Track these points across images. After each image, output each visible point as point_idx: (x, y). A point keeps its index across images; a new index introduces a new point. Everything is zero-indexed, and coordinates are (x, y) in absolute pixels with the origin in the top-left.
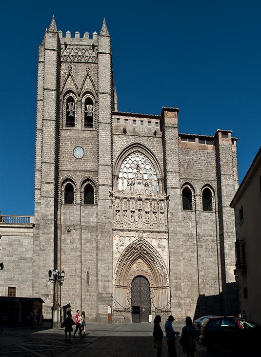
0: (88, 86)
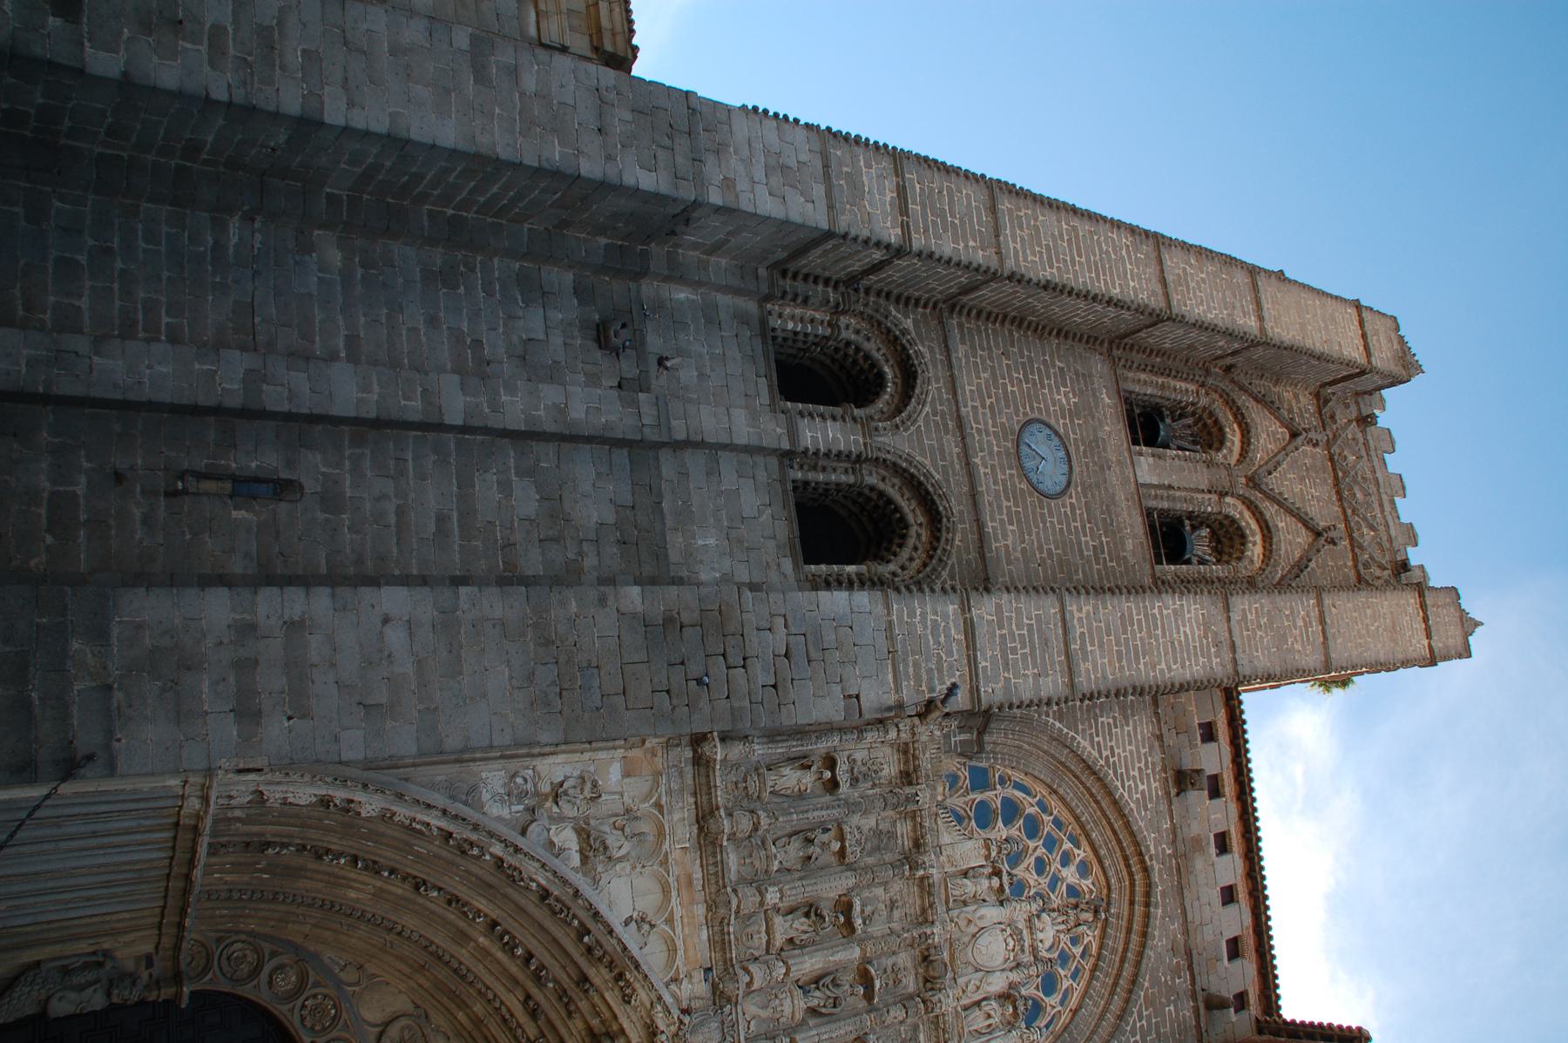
0: (1291, 539)
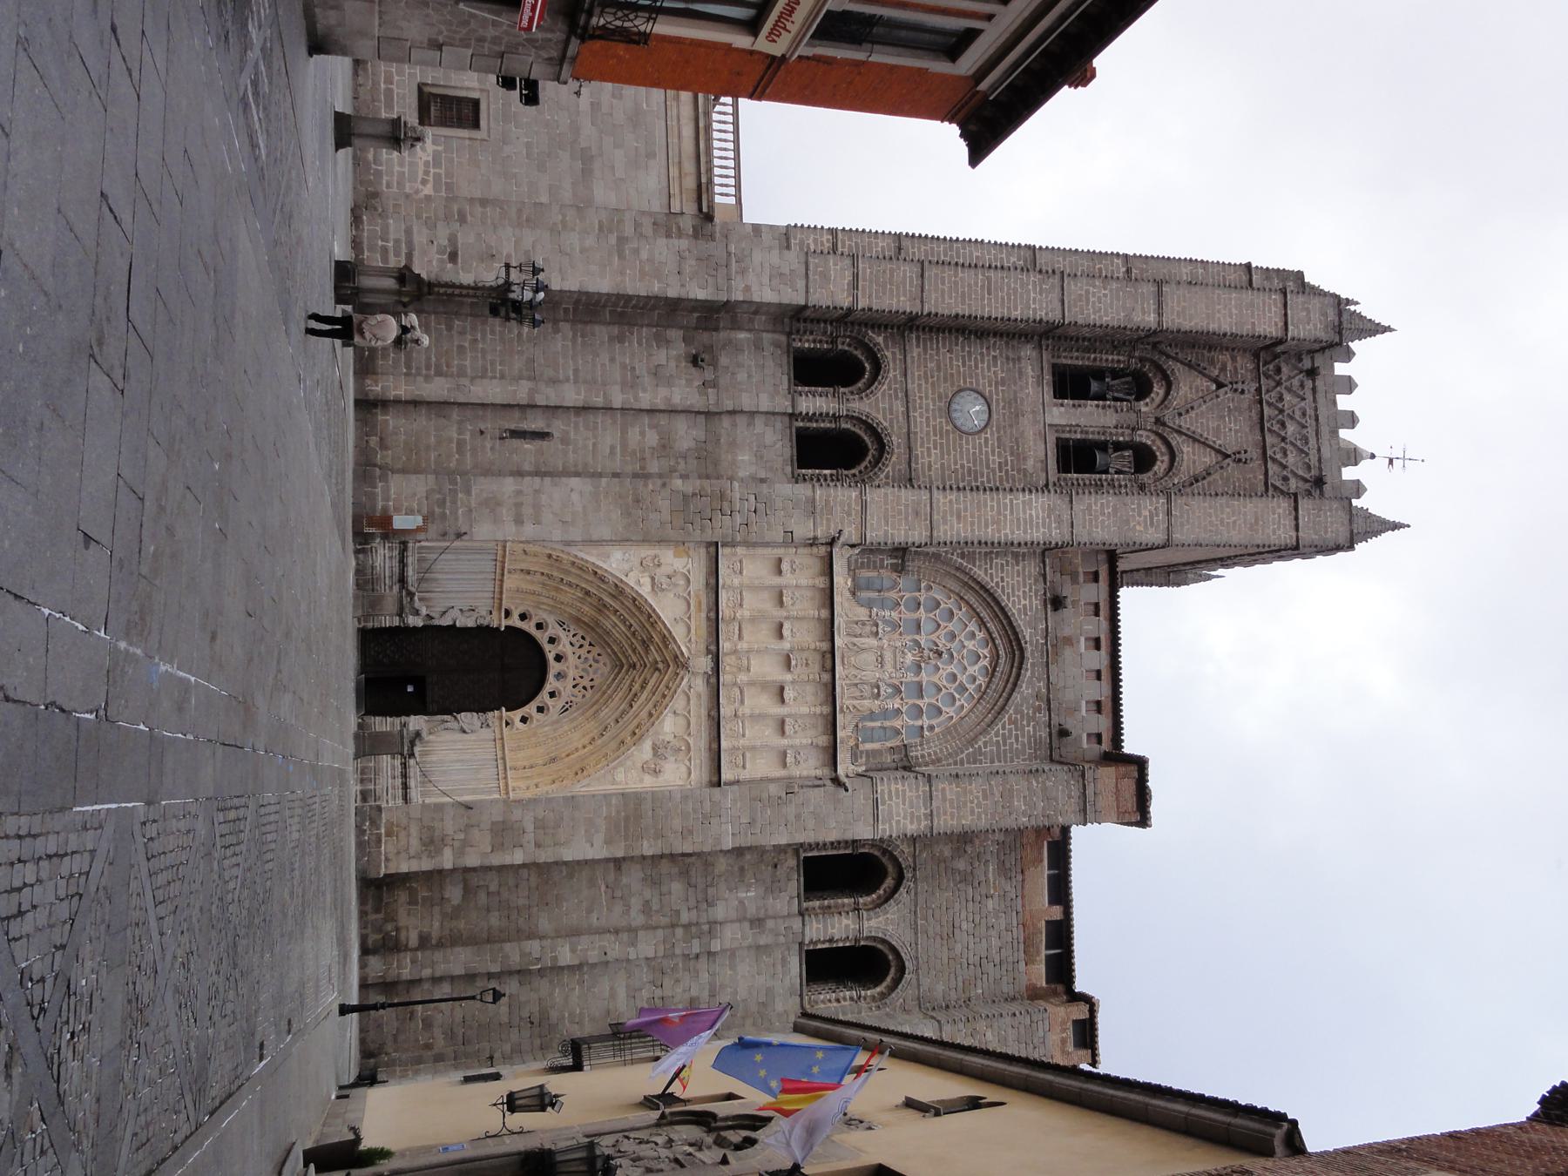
0: (1192, 458)
